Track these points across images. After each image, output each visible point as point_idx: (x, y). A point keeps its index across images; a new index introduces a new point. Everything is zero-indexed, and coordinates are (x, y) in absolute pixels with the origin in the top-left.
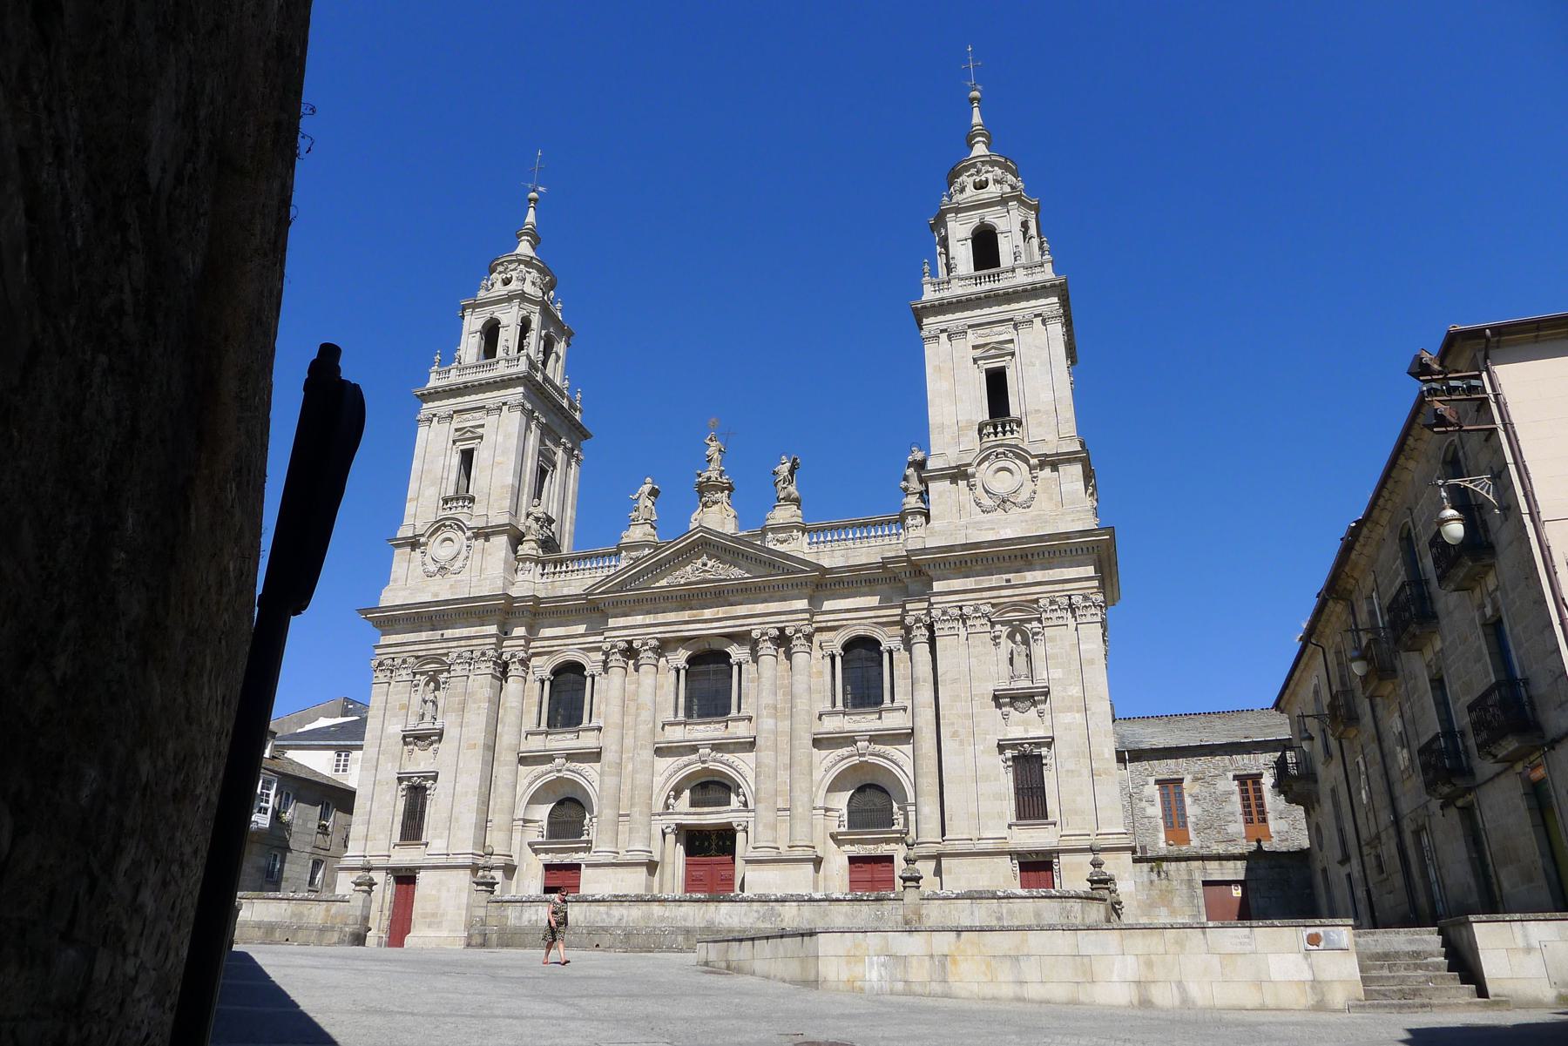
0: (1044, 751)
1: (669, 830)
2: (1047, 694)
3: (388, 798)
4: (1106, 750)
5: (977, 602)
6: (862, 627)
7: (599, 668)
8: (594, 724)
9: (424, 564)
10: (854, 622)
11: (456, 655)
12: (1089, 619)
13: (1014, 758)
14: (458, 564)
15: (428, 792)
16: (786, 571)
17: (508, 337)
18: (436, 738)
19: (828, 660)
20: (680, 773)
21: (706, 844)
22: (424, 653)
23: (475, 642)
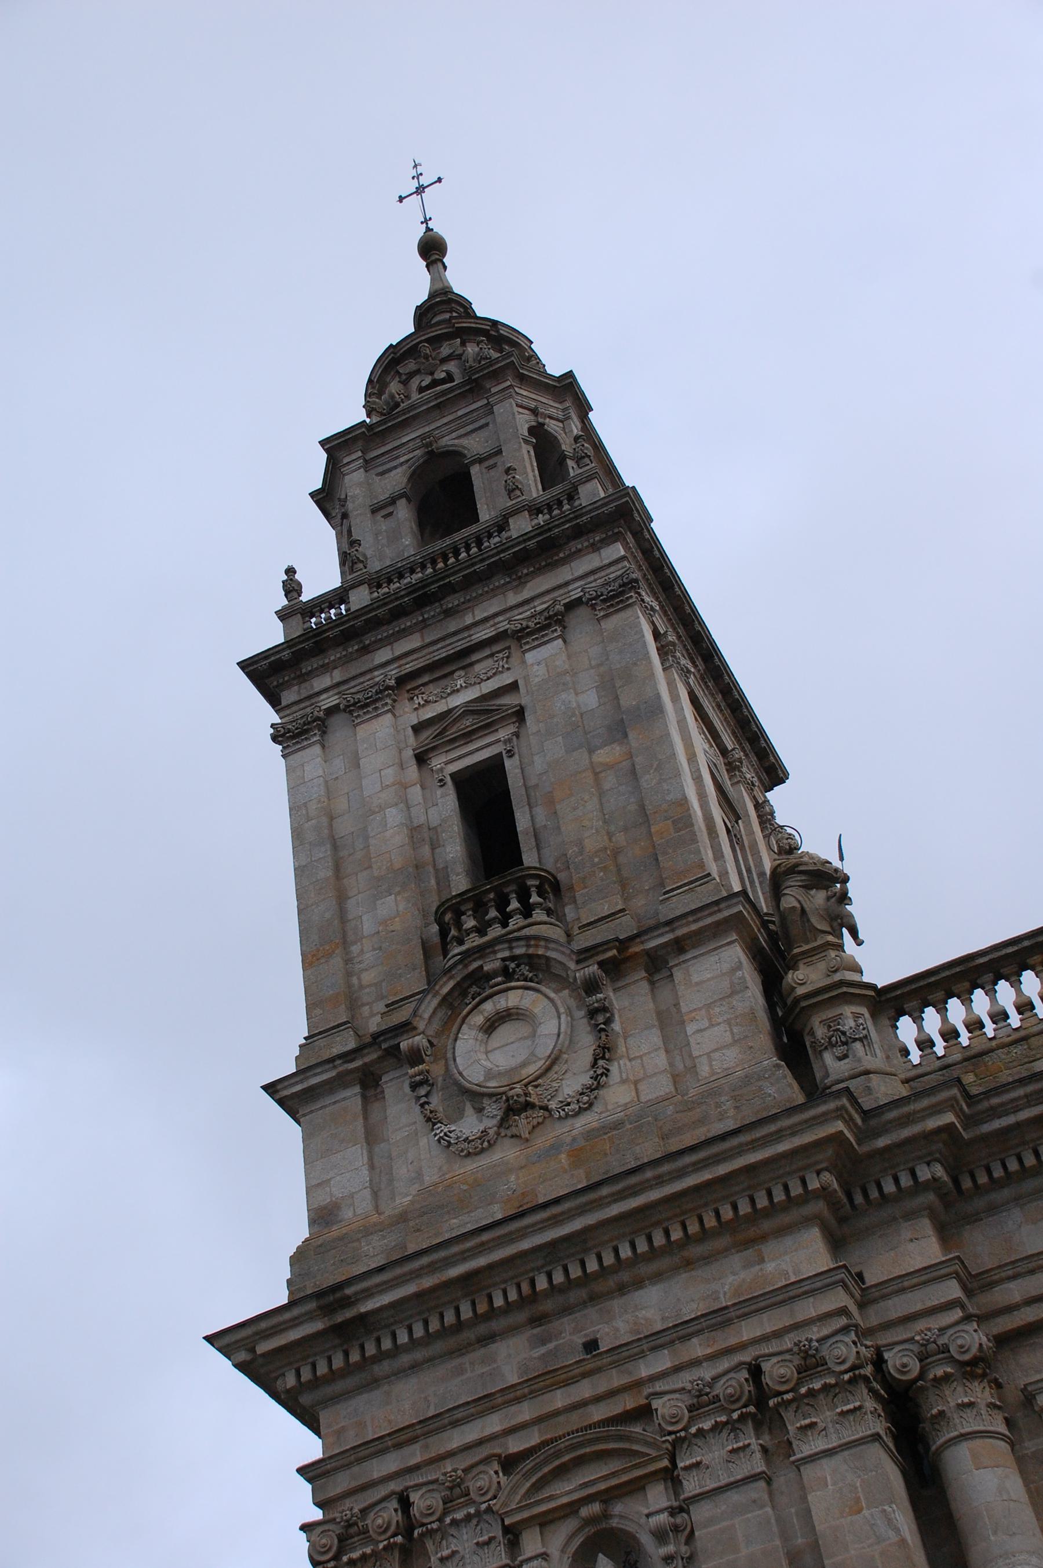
22: (533, 1438)
23: (748, 1330)
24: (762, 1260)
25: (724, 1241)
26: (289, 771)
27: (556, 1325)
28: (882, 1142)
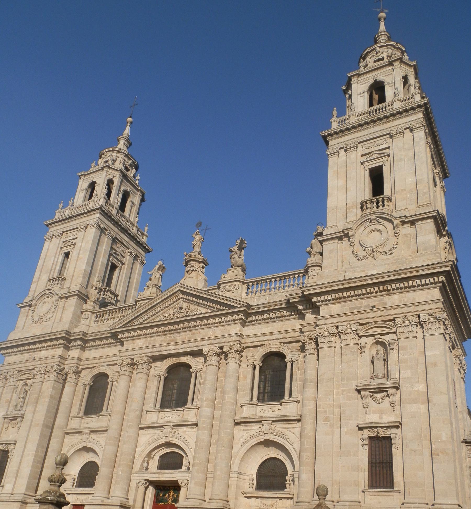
0: (392, 432)
6: (274, 346)
8: (108, 412)
10: (270, 342)
11: (38, 369)
12: (433, 331)
13: (371, 438)
19: (251, 369)
24: (55, 352)
28: (74, 338)
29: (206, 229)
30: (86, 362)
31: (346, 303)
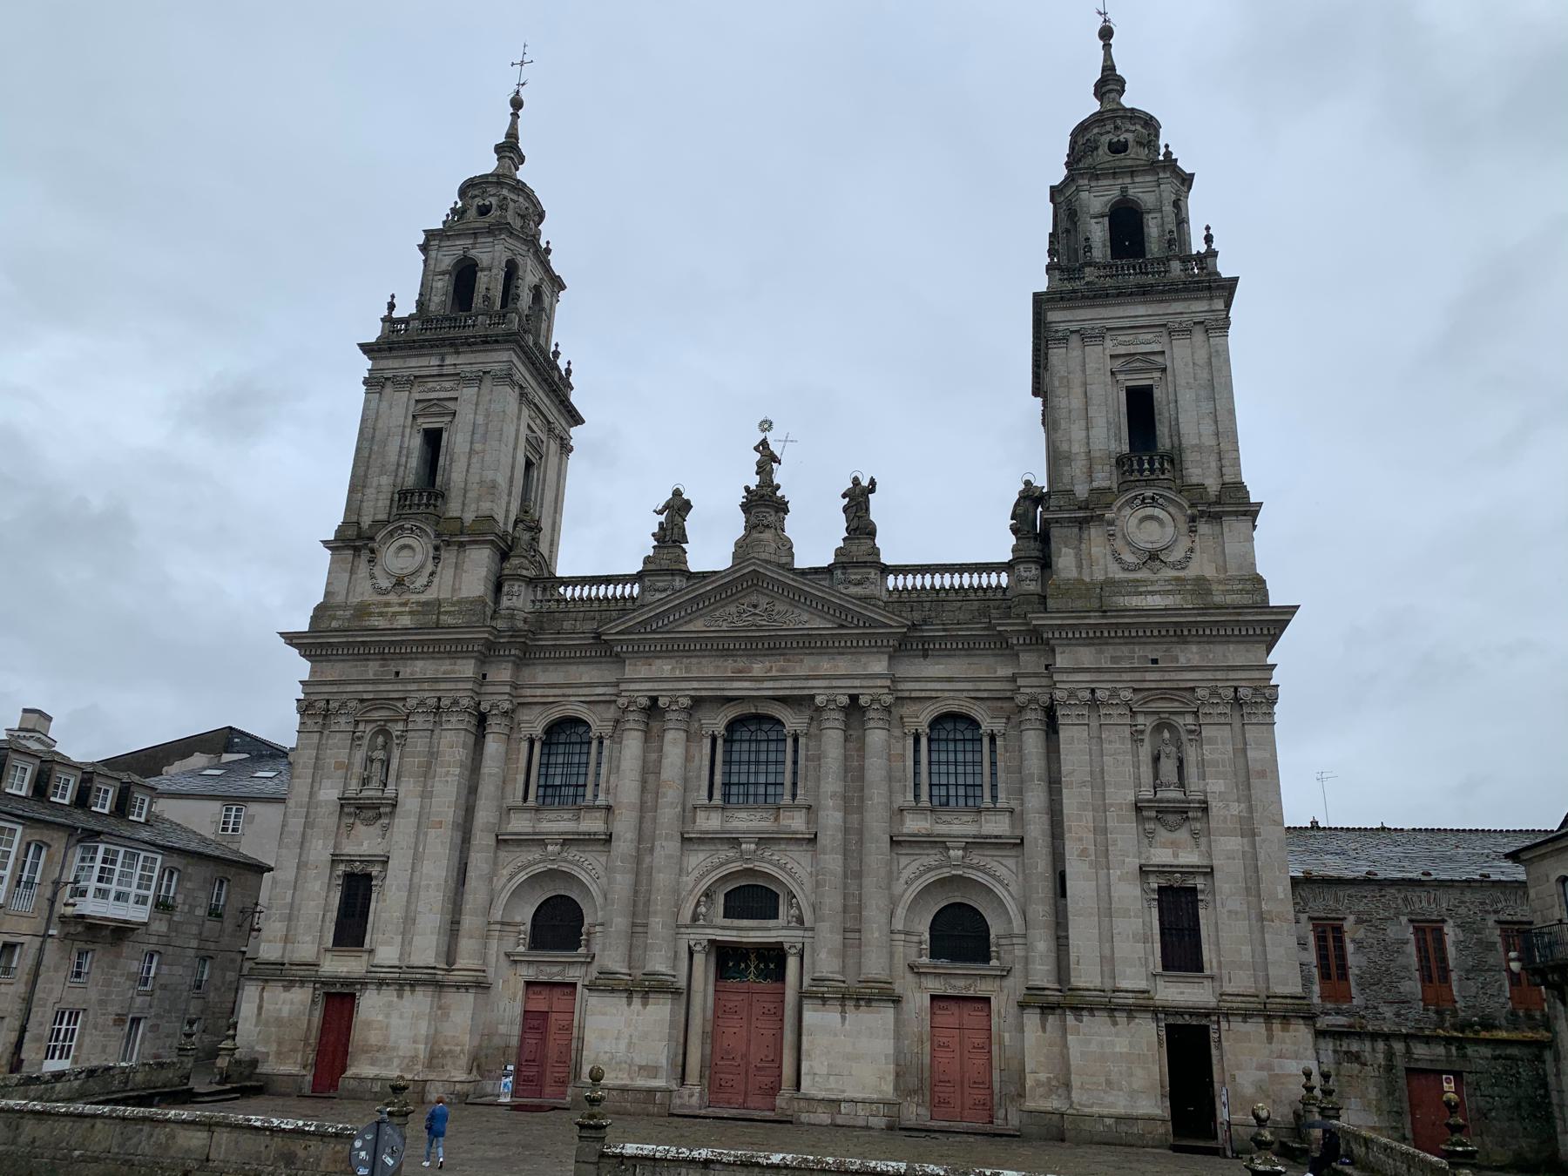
0: (1200, 883)
1: (698, 948)
2: (1205, 810)
3: (317, 888)
4: (1280, 889)
5: (1114, 685)
6: (957, 702)
7: (607, 730)
9: (372, 577)
10: (947, 694)
11: (415, 702)
13: (1161, 890)
14: (422, 580)
15: (373, 883)
16: (861, 624)
17: (489, 283)
18: (388, 810)
19: (910, 741)
20: (714, 873)
21: (743, 965)
23: (443, 686)
24: (455, 664)
25: (446, 655)
26: (366, 400)
27: (389, 662)
29: (786, 441)
30: (528, 692)
31: (1105, 647)
